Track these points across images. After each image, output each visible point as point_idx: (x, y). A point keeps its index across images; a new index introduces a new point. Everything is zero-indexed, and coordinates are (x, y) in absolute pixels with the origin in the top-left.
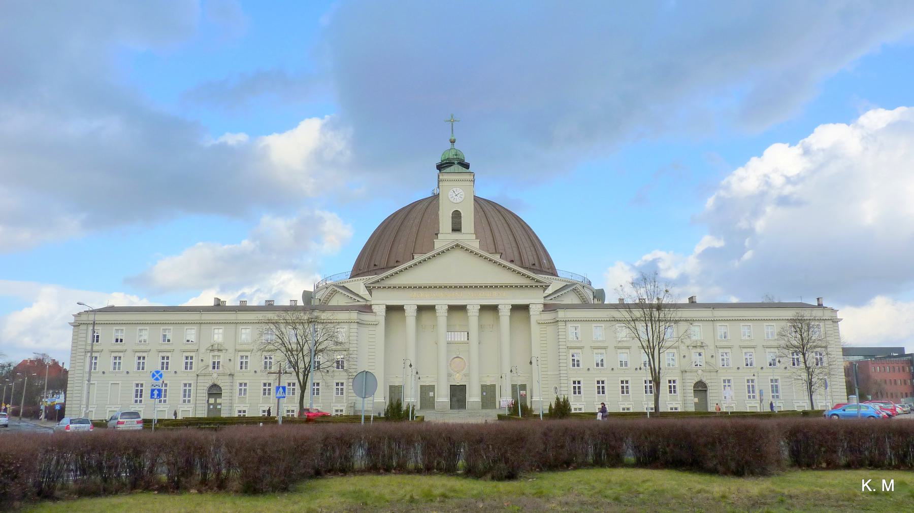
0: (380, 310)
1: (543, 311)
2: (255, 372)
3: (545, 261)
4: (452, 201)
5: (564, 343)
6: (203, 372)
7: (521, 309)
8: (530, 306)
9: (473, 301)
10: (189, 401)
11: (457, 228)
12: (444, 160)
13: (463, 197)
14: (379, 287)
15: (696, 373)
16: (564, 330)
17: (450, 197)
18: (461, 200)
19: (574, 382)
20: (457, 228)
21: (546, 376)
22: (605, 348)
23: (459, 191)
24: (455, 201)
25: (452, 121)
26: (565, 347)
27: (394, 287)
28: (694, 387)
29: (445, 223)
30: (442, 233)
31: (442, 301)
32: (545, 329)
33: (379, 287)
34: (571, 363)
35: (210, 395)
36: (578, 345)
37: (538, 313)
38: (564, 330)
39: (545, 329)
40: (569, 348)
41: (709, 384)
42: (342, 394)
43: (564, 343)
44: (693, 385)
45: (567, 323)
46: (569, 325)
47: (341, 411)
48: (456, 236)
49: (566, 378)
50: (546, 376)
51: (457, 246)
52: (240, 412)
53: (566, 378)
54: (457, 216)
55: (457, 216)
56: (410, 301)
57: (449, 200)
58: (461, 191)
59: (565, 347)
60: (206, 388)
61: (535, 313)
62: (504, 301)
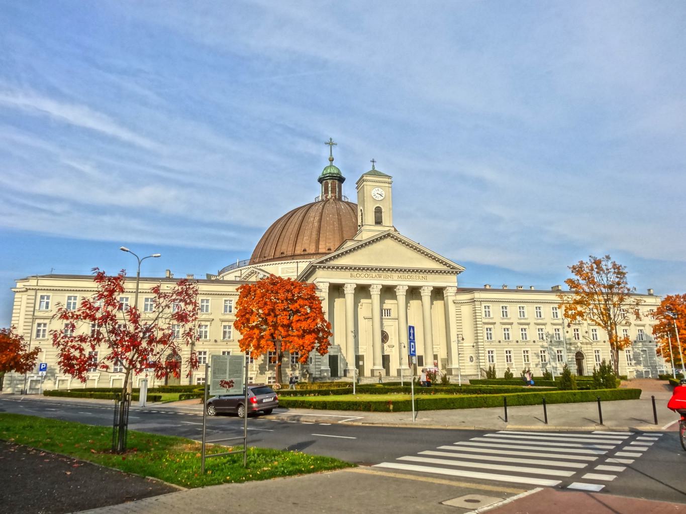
1: (457, 293)
2: (216, 341)
4: (374, 197)
5: (480, 320)
7: (438, 293)
9: (402, 284)
11: (378, 222)
12: (326, 174)
14: (324, 267)
16: (480, 309)
20: (378, 222)
22: (528, 324)
23: (380, 191)
24: (376, 199)
26: (481, 323)
27: (338, 268)
29: (370, 218)
31: (377, 282)
32: (459, 308)
36: (491, 321)
37: (454, 294)
38: (480, 309)
39: (459, 308)
40: (485, 323)
43: (480, 320)
45: (482, 302)
46: (484, 304)
48: (379, 228)
49: (483, 349)
51: (389, 235)
52: (199, 379)
53: (483, 349)
54: (378, 211)
55: (378, 211)
56: (350, 282)
57: (373, 198)
58: (382, 190)
59: (481, 323)
61: (451, 294)
62: (427, 284)
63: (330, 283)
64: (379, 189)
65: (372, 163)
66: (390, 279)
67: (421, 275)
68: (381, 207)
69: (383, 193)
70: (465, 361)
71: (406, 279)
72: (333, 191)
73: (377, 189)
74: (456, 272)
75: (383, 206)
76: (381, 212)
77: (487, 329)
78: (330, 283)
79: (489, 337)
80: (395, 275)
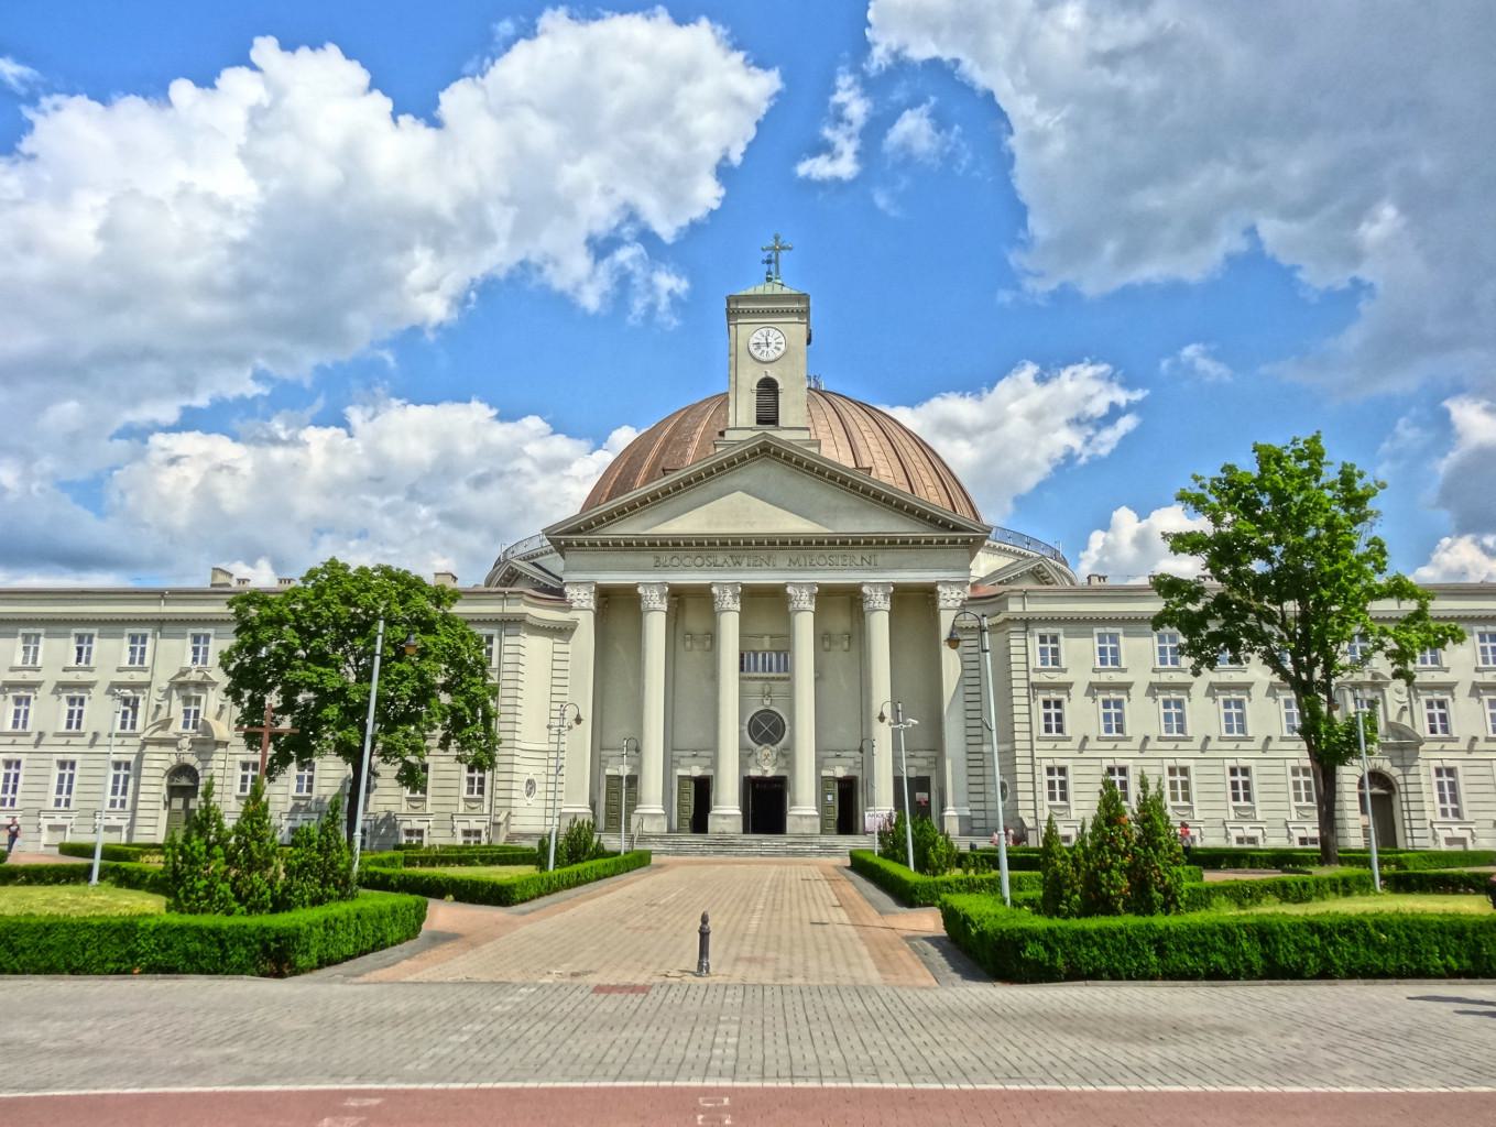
0: (582, 599)
4: (757, 354)
6: (159, 734)
8: (939, 588)
10: (123, 803)
13: (783, 347)
17: (752, 348)
18: (779, 354)
19: (1050, 771)
21: (980, 756)
23: (774, 336)
24: (764, 358)
30: (735, 429)
33: (580, 545)
34: (1042, 723)
35: (173, 791)
37: (958, 604)
40: (1035, 687)
42: (481, 791)
47: (478, 833)
50: (980, 756)
54: (768, 387)
55: (768, 387)
60: (162, 773)
61: (950, 604)
63: (597, 586)
64: (772, 331)
65: (766, 266)
66: (765, 566)
67: (858, 555)
68: (771, 374)
69: (782, 339)
70: (514, 794)
71: (812, 567)
73: (764, 331)
74: (966, 542)
75: (782, 376)
76: (776, 393)
77: (1047, 704)
78: (597, 586)
79: (1056, 724)
80: (782, 558)
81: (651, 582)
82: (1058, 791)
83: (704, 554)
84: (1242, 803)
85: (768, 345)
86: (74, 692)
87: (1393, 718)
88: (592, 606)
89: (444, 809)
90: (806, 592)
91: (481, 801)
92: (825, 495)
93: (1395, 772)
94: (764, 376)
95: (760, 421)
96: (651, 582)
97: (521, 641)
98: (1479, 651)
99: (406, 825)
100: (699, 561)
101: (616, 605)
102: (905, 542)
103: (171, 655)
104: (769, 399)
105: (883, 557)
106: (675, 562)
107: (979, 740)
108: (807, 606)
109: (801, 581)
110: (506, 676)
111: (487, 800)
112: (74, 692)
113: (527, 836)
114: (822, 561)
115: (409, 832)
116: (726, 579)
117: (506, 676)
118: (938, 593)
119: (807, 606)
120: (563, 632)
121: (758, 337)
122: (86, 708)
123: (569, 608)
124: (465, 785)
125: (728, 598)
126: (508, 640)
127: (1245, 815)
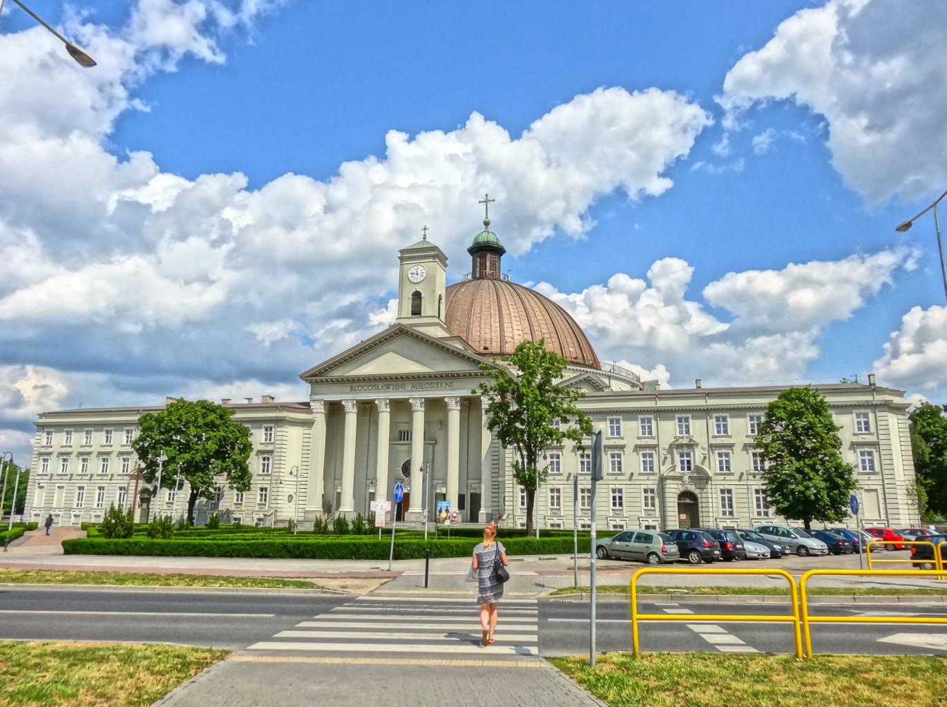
3: (571, 349)
4: (412, 279)
11: (416, 312)
13: (424, 275)
15: (680, 482)
17: (410, 276)
20: (416, 312)
24: (415, 281)
25: (486, 202)
28: (679, 499)
41: (699, 496)
44: (676, 496)
69: (424, 271)
71: (422, 389)
72: (493, 265)
78: (325, 401)
81: (349, 399)
82: (617, 501)
83: (373, 384)
84: (618, 507)
85: (417, 274)
86: (104, 455)
87: (698, 463)
88: (323, 411)
89: (249, 508)
90: (419, 402)
91: (265, 505)
92: (430, 353)
93: (697, 491)
94: (414, 290)
95: (413, 314)
96: (349, 399)
97: (285, 429)
98: (715, 427)
99: (234, 516)
100: (370, 388)
101: (335, 411)
102: (470, 375)
103: (120, 440)
104: (417, 302)
105: (456, 384)
106: (360, 388)
107: (496, 475)
108: (419, 409)
109: (416, 397)
110: (277, 446)
111: (267, 505)
112: (104, 455)
113: (282, 521)
114: (427, 386)
115: (236, 519)
116: (381, 397)
117: (277, 446)
118: (481, 401)
119: (419, 409)
120: (308, 424)
121: (413, 270)
122: (88, 463)
123: (312, 413)
124: (259, 497)
125: (383, 406)
126: (279, 429)
127: (618, 514)
